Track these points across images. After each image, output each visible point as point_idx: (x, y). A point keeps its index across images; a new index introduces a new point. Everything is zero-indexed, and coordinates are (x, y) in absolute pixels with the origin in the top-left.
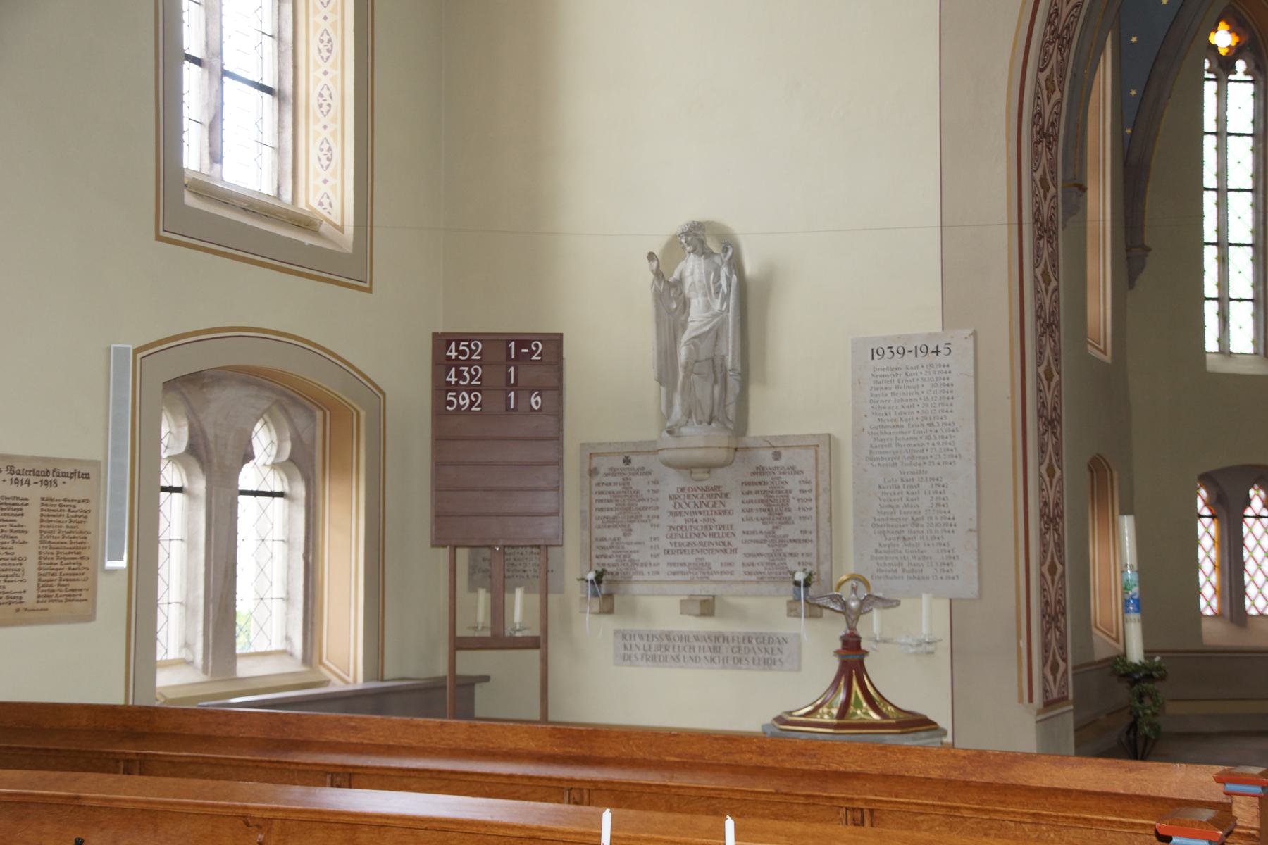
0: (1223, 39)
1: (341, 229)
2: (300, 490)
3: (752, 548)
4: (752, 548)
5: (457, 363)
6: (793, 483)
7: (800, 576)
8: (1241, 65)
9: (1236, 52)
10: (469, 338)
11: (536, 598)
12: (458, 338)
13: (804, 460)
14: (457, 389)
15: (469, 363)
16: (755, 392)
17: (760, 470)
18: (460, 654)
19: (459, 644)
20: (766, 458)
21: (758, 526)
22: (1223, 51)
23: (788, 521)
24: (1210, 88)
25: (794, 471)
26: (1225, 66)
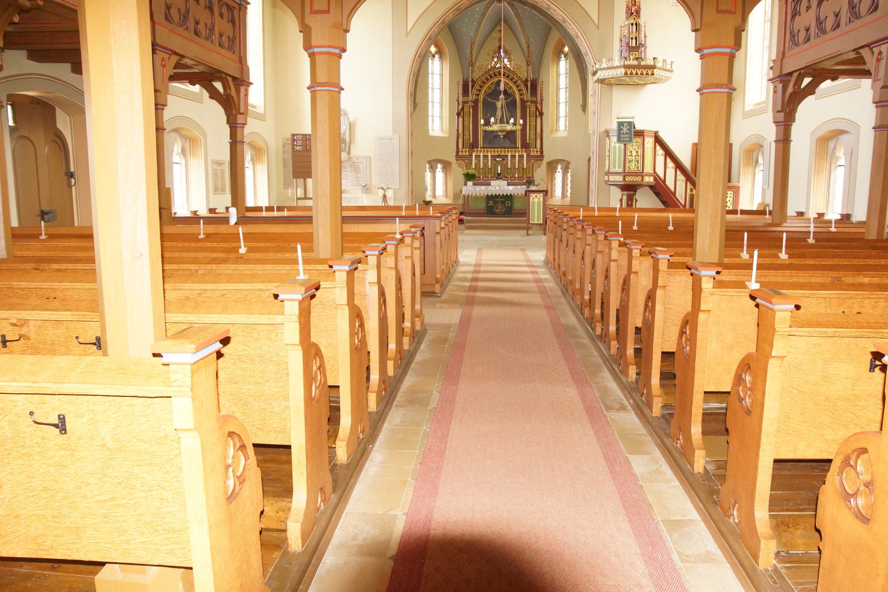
0: (433, 49)
1: (261, 107)
2: (184, 162)
3: (352, 179)
4: (352, 179)
5: (296, 140)
6: (361, 165)
7: (364, 185)
8: (437, 56)
9: (436, 53)
10: (299, 135)
11: (303, 191)
12: (296, 135)
13: (364, 161)
14: (297, 146)
15: (299, 140)
16: (352, 146)
17: (354, 163)
18: (298, 201)
19: (298, 199)
20: (355, 160)
21: (353, 174)
22: (433, 52)
23: (360, 173)
24: (430, 61)
25: (361, 163)
26: (434, 56)
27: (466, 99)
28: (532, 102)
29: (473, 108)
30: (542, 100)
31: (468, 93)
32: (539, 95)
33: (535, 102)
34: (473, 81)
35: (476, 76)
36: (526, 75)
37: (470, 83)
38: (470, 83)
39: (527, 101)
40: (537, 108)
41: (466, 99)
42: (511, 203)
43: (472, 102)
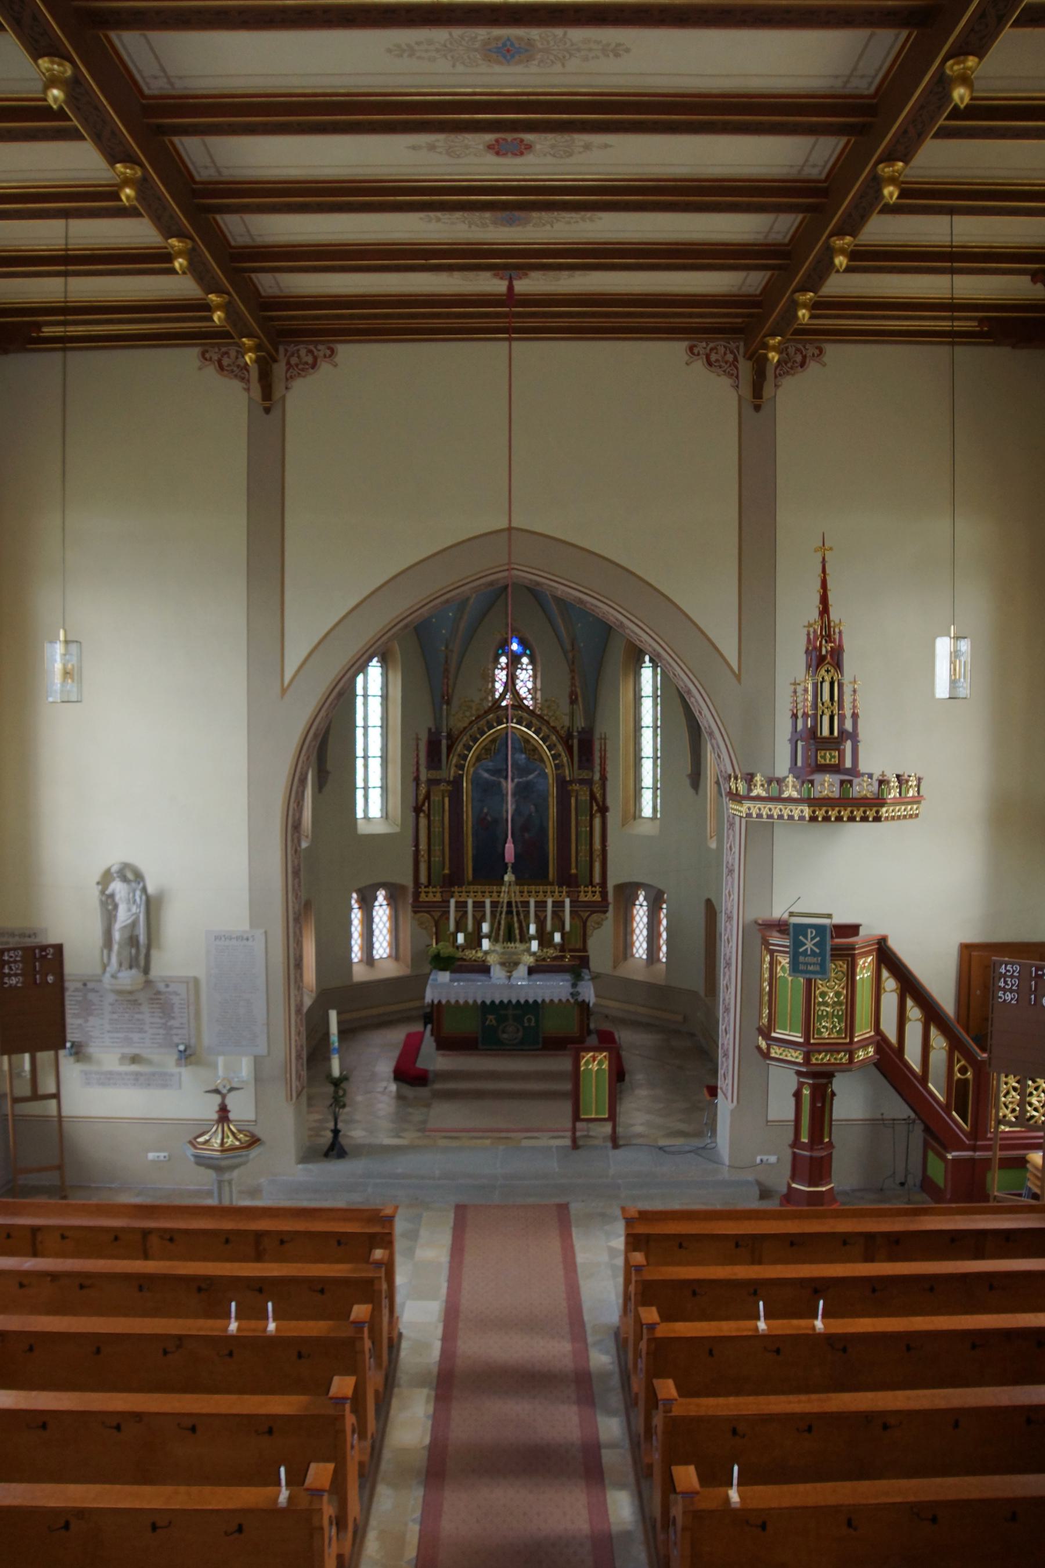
27: (434, 775)
28: (582, 782)
29: (450, 797)
30: (604, 778)
31: (440, 760)
32: (597, 768)
33: (589, 782)
34: (449, 736)
35: (458, 722)
36: (567, 722)
37: (444, 742)
38: (444, 742)
39: (571, 782)
40: (593, 797)
41: (434, 775)
42: (537, 1021)
43: (449, 782)
